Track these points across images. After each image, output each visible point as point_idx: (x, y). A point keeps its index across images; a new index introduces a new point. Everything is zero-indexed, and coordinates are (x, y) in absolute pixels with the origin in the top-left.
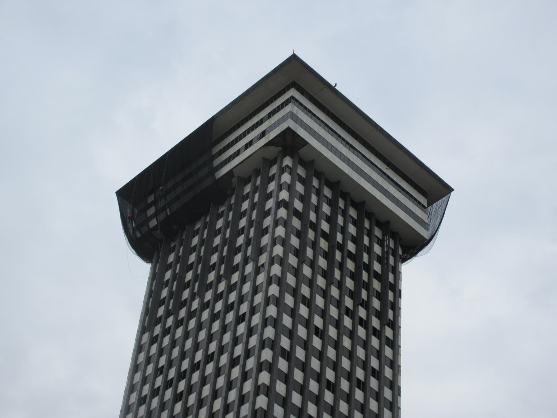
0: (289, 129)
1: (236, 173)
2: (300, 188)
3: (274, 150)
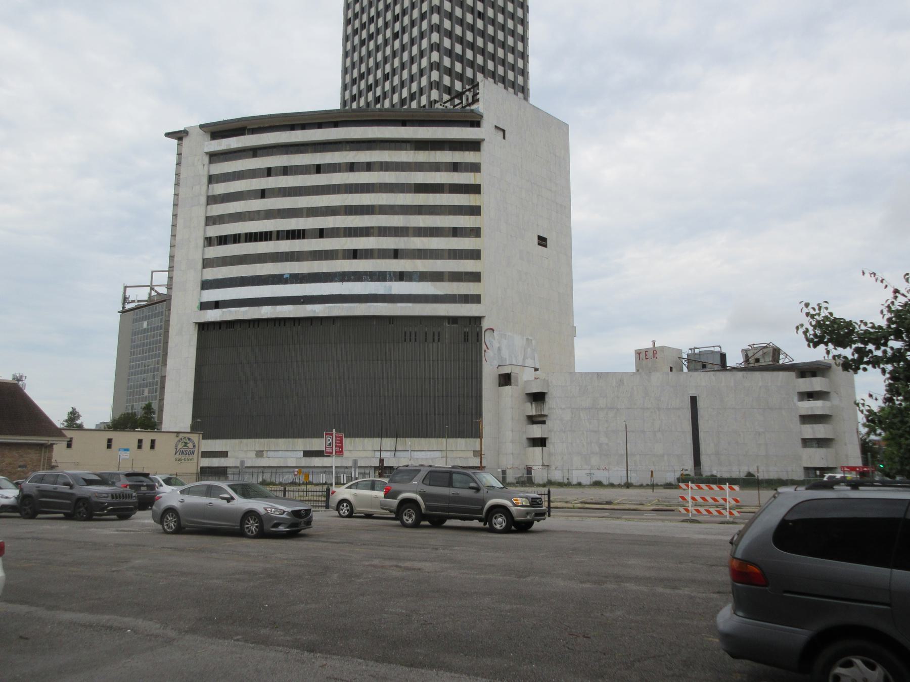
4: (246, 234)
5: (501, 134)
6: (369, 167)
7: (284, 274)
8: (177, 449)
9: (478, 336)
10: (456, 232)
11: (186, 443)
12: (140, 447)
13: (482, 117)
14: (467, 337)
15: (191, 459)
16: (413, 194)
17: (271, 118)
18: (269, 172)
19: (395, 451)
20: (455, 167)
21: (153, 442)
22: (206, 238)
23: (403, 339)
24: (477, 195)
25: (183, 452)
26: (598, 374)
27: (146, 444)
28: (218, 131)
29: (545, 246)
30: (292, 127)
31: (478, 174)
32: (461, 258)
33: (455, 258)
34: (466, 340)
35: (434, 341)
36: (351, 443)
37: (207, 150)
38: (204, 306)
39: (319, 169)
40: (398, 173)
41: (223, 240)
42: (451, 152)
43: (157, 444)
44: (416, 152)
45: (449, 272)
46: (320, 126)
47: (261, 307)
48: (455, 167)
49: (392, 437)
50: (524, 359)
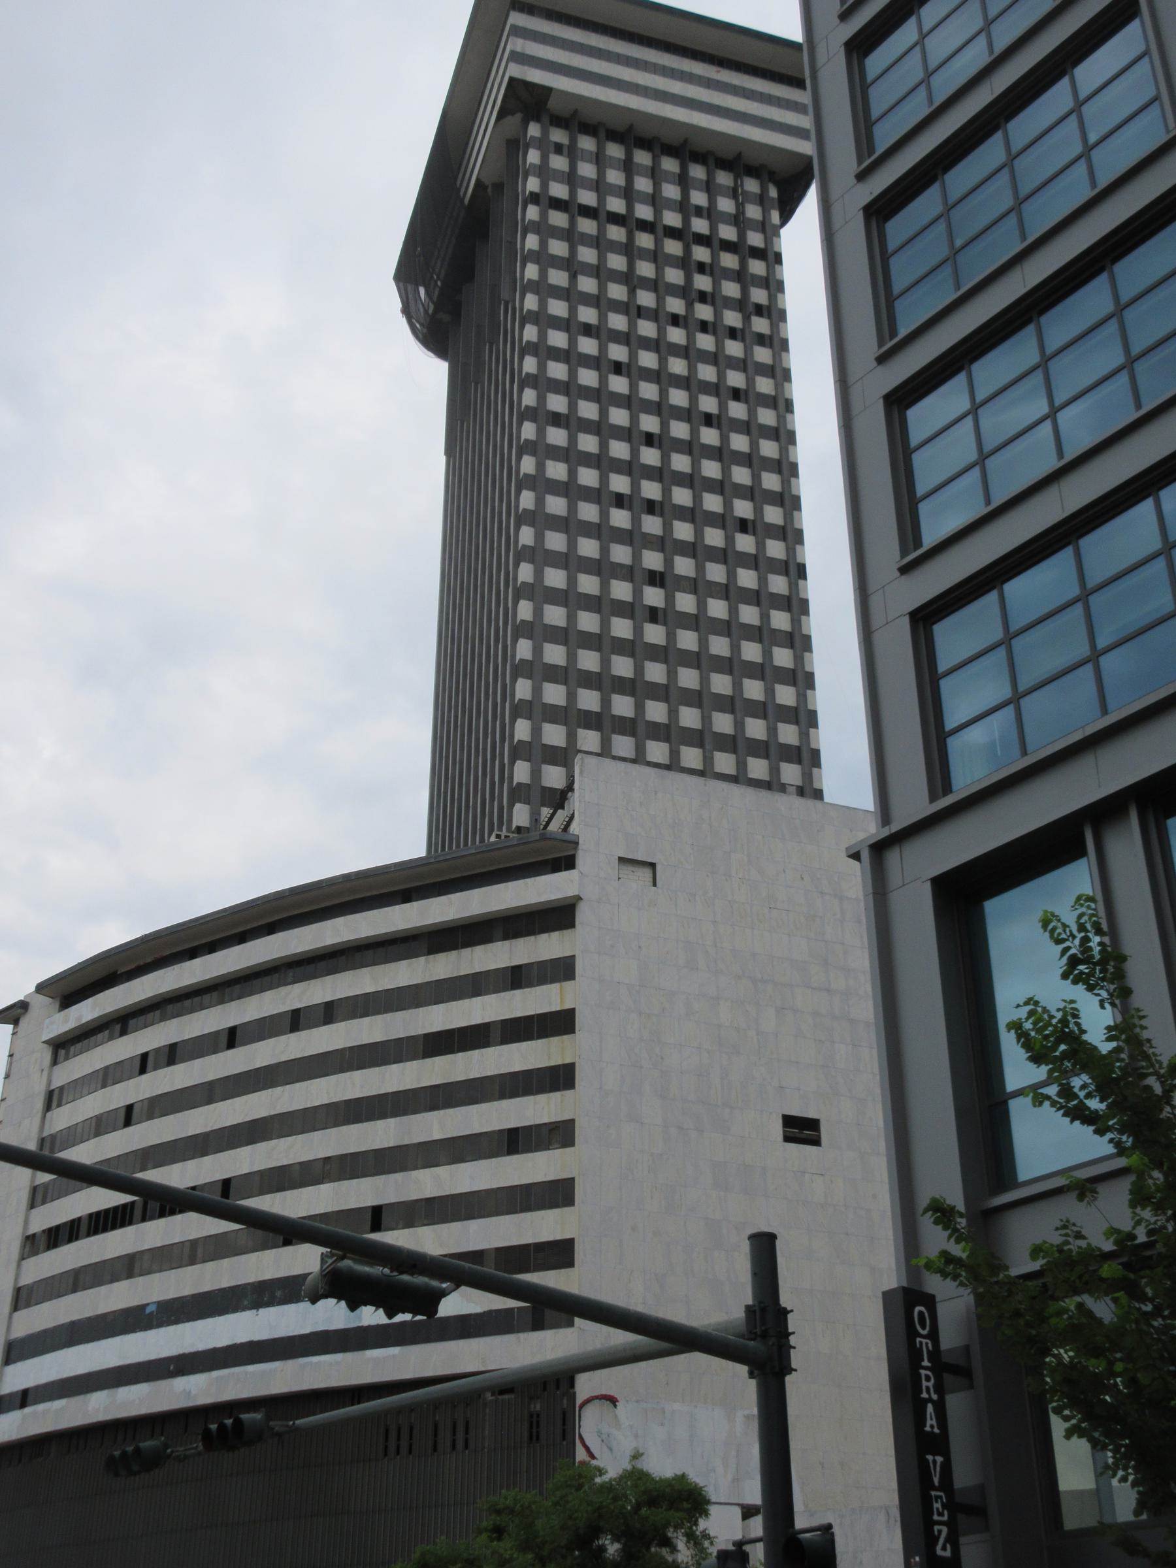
0: (511, 79)
1: (487, 181)
2: (559, 163)
3: (515, 120)
4: (91, 1215)
5: (646, 873)
6: (329, 1013)
7: (148, 1304)
9: (564, 1424)
13: (577, 843)
14: (538, 1423)
16: (420, 1061)
18: (144, 1064)
22: (28, 1238)
24: (566, 1037)
29: (816, 1142)
30: (193, 953)
31: (568, 985)
34: (534, 1438)
35: (454, 1447)
37: (45, 1038)
39: (232, 1038)
41: (57, 1237)
42: (506, 944)
45: (498, 1250)
46: (242, 938)
47: (88, 1395)
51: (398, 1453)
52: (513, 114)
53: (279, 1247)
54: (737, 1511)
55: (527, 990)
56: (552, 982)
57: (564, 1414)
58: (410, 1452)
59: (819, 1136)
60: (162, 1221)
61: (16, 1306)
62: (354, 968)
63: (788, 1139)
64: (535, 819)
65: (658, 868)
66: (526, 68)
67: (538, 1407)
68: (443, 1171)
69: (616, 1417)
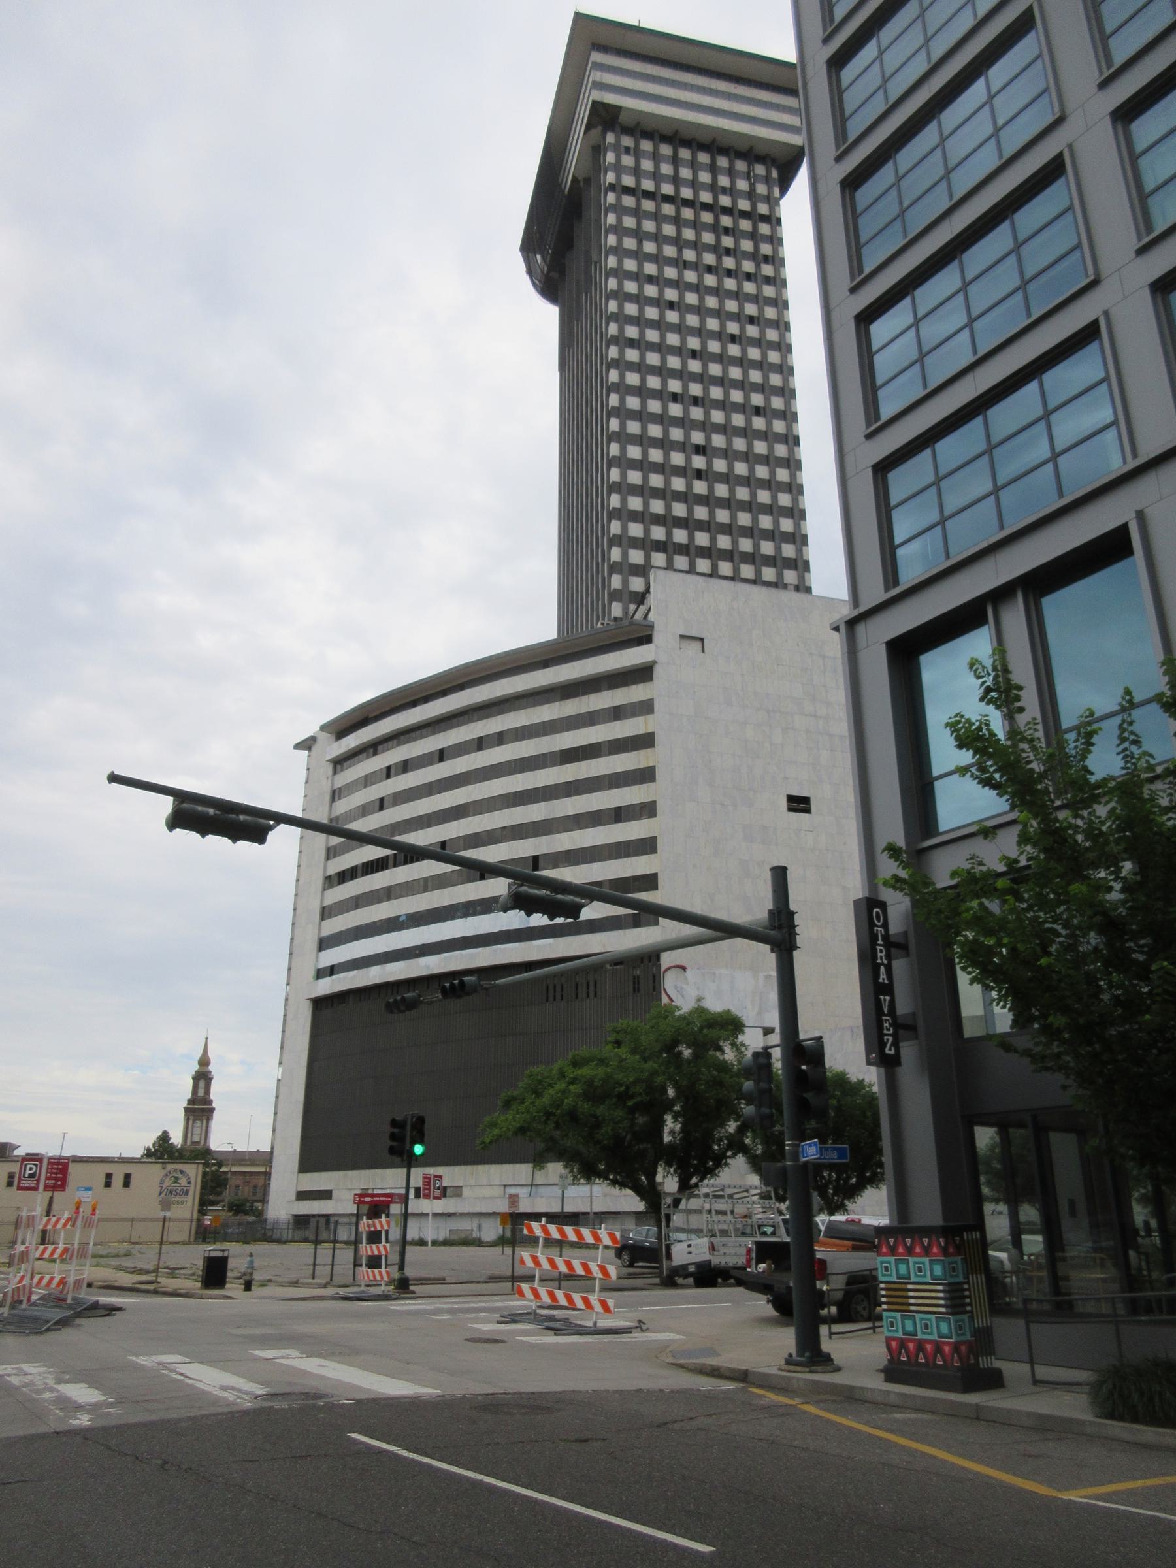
0: (595, 104)
2: (628, 161)
3: (596, 132)
4: (363, 864)
5: (698, 645)
6: (500, 739)
7: (400, 916)
8: (162, 1187)
9: (654, 982)
10: (619, 815)
11: (177, 1178)
12: (108, 1184)
13: (653, 627)
14: (638, 984)
15: (182, 1203)
17: (393, 694)
18: (388, 772)
19: (532, 1185)
20: (617, 713)
21: (127, 1178)
23: (574, 997)
25: (171, 1192)
26: (852, 1031)
27: (118, 1181)
28: (343, 727)
29: (808, 811)
30: (414, 704)
31: (650, 717)
32: (628, 855)
33: (619, 856)
35: (588, 996)
36: (472, 1174)
37: (328, 758)
38: (320, 974)
39: (442, 755)
40: (537, 739)
43: (133, 1182)
44: (562, 702)
45: (611, 880)
47: (369, 969)
48: (617, 713)
49: (528, 1162)
50: (759, 1013)
51: (555, 999)
52: (595, 126)
53: (477, 881)
54: (761, 1031)
55: (624, 721)
56: (639, 716)
57: (654, 977)
58: (562, 999)
59: (810, 808)
60: (406, 867)
61: (323, 918)
62: (515, 710)
63: (790, 809)
64: (626, 612)
65: (705, 641)
66: (603, 93)
67: (638, 972)
68: (575, 834)
69: (686, 978)
